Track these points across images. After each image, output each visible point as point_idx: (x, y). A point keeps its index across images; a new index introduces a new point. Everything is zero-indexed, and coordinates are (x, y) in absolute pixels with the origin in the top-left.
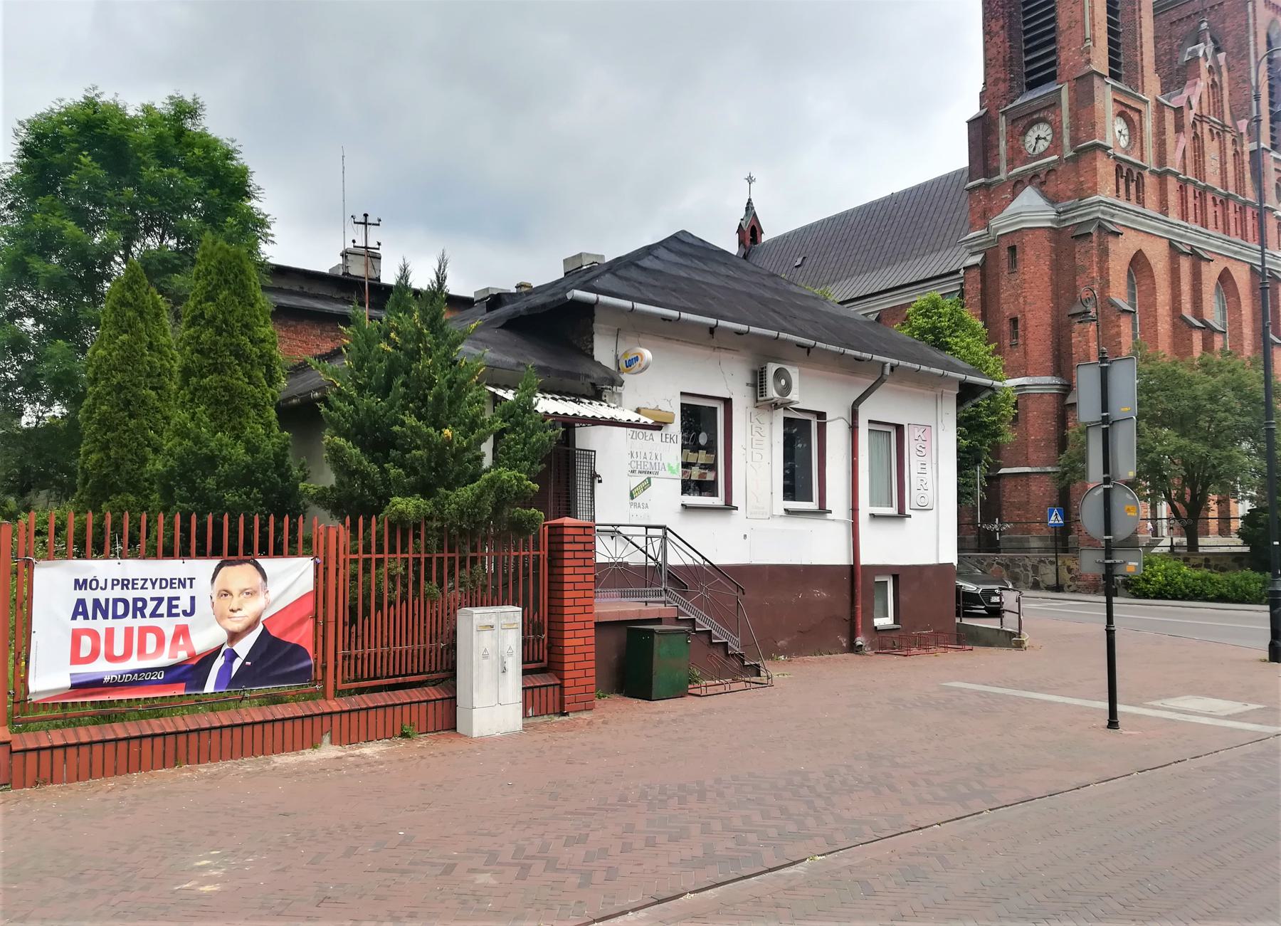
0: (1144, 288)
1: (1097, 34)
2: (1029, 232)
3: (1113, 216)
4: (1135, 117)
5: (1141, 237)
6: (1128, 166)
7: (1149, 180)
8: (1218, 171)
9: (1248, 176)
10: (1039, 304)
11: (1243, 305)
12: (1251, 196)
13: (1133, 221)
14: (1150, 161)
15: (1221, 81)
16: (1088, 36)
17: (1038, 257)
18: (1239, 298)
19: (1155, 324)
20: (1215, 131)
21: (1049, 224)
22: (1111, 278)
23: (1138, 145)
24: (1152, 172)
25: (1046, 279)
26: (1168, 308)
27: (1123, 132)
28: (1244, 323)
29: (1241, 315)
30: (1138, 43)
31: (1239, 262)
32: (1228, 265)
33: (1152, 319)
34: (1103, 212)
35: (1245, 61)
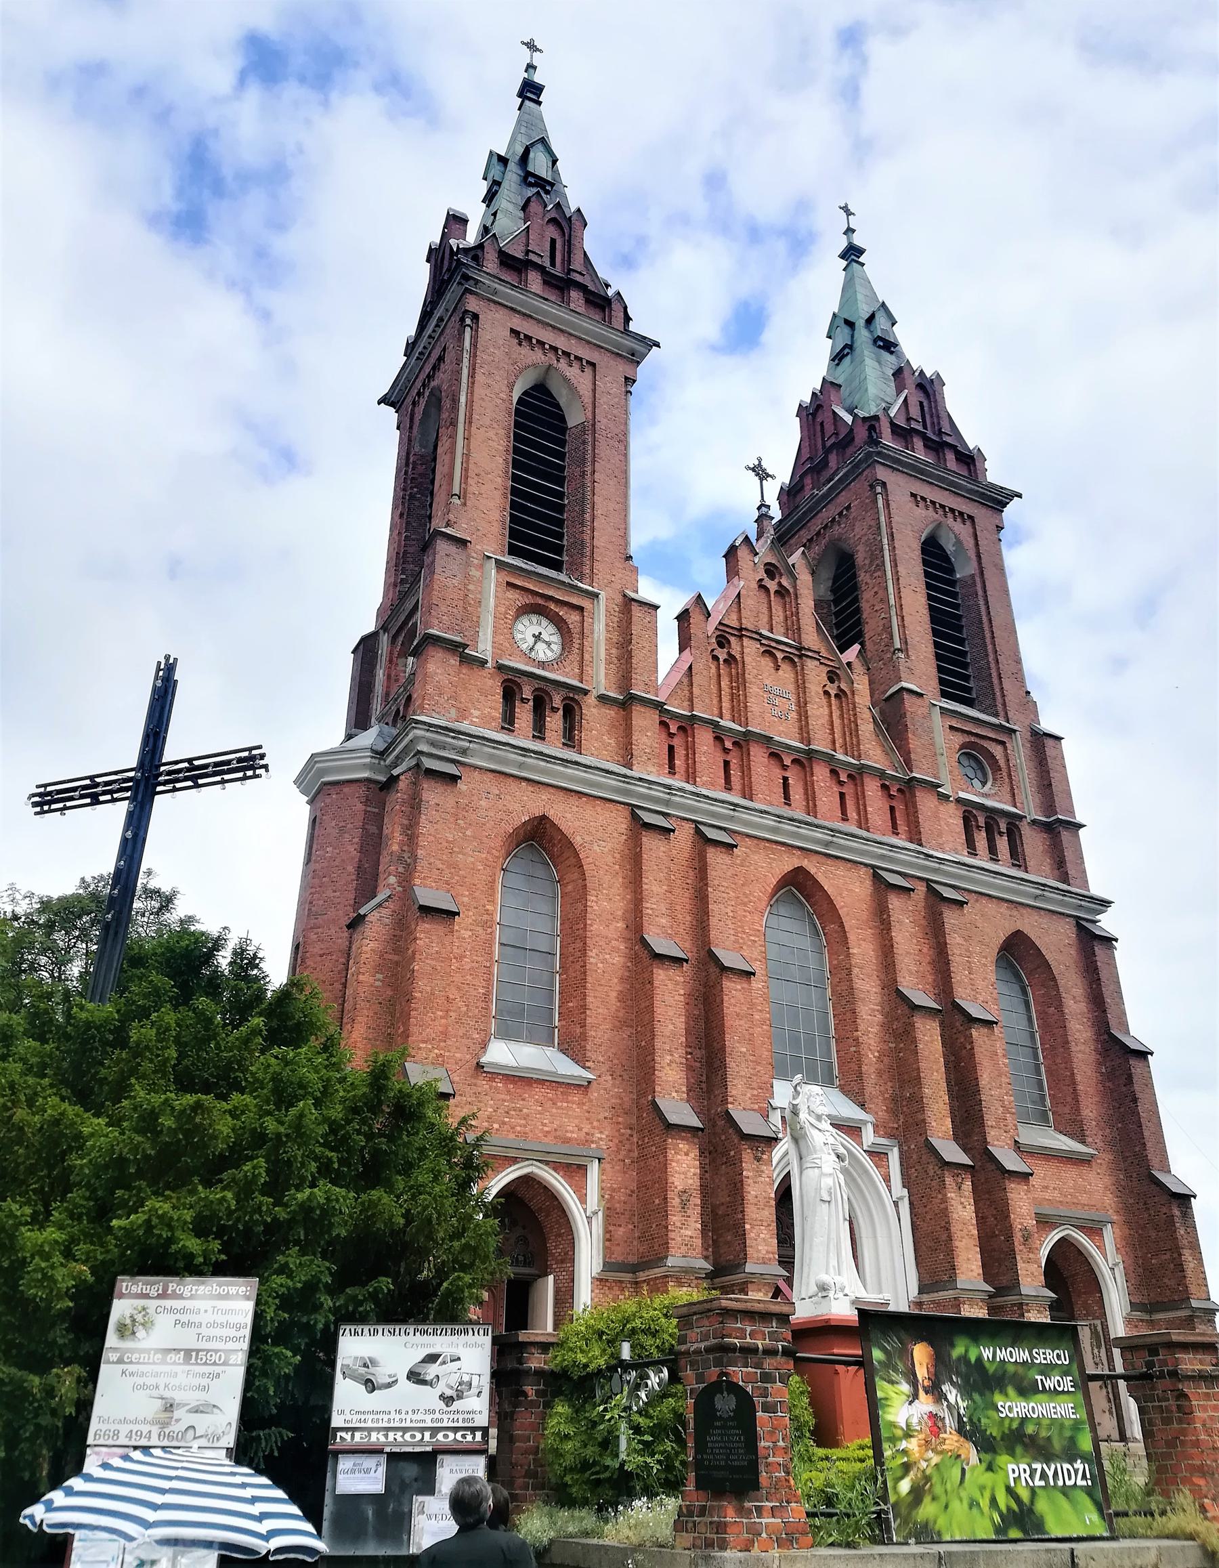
0: (570, 887)
1: (473, 488)
2: (333, 790)
3: (464, 752)
4: (572, 618)
5: (545, 795)
6: (564, 692)
7: (594, 717)
8: (793, 715)
9: (866, 728)
10: (332, 913)
11: (852, 937)
12: (874, 755)
13: (521, 766)
14: (601, 679)
15: (795, 587)
16: (456, 490)
17: (342, 830)
18: (842, 925)
19: (584, 951)
20: (780, 655)
21: (365, 775)
22: (420, 853)
23: (575, 657)
24: (602, 698)
25: (350, 869)
26: (621, 925)
27: (545, 636)
28: (855, 971)
29: (848, 955)
30: (587, 516)
31: (840, 863)
32: (805, 863)
33: (579, 945)
34: (433, 744)
35: (879, 573)
